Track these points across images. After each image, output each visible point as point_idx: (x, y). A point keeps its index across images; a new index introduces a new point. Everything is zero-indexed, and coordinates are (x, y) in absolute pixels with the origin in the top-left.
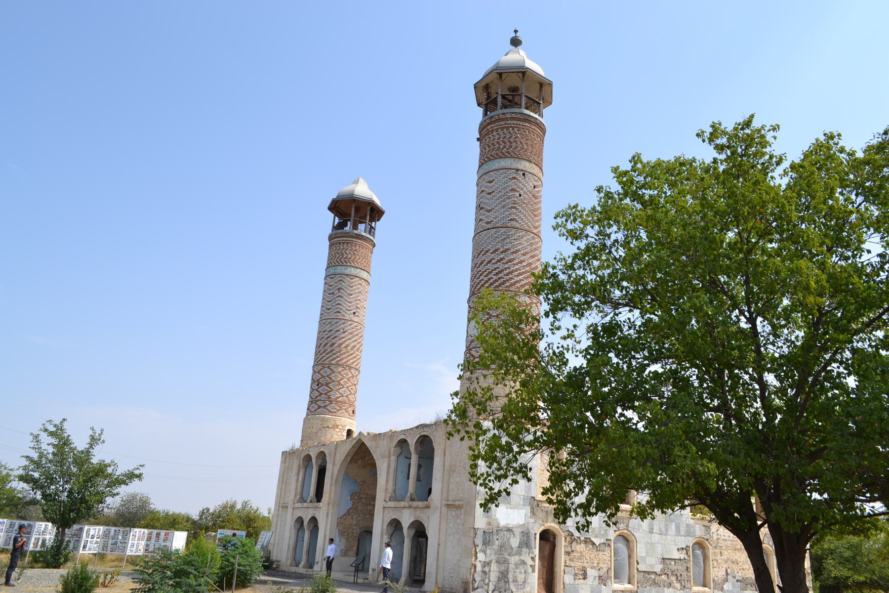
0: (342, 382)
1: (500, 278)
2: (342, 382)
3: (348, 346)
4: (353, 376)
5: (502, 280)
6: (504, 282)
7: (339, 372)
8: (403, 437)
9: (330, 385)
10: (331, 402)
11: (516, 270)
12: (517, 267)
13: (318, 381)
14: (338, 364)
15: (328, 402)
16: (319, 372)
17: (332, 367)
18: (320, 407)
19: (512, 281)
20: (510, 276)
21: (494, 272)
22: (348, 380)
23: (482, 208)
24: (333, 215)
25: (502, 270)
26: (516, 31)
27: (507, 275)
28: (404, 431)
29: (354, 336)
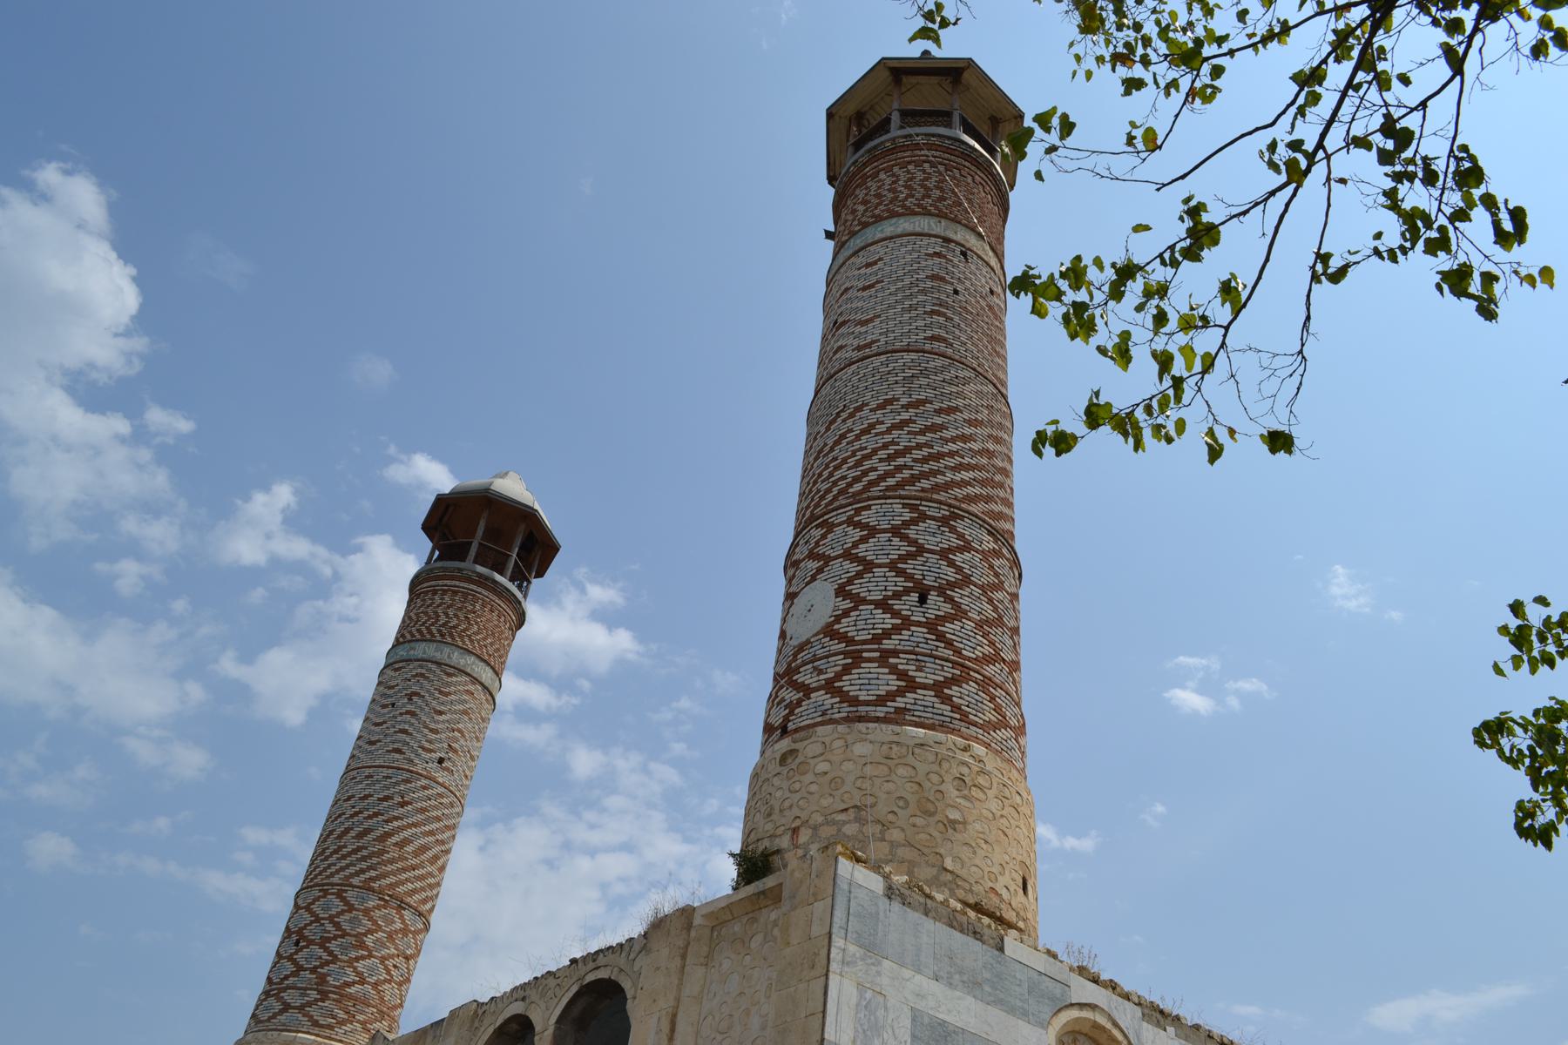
0: (369, 940)
1: (899, 469)
2: (369, 940)
3: (406, 842)
4: (405, 931)
5: (906, 474)
6: (913, 480)
7: (367, 912)
8: (517, 1008)
9: (333, 945)
10: (324, 996)
11: (951, 454)
12: (952, 447)
14: (367, 887)
15: (314, 995)
17: (350, 895)
18: (287, 1007)
19: (940, 479)
20: (933, 465)
21: (882, 454)
22: (390, 937)
24: (430, 545)
25: (908, 450)
27: (925, 460)
28: (524, 986)
29: (428, 821)
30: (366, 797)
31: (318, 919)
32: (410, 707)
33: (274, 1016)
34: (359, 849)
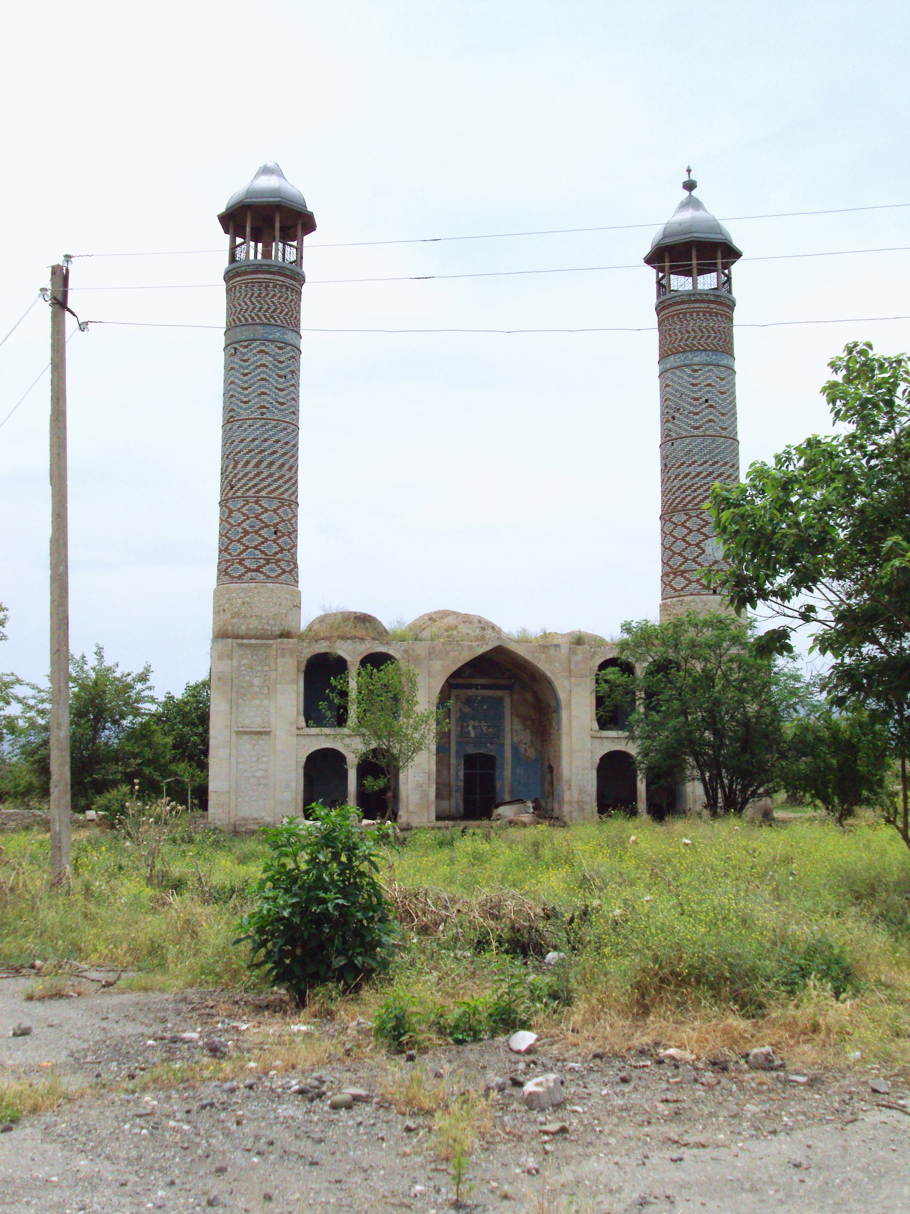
13: (275, 525)
16: (275, 511)
18: (284, 572)
23: (711, 406)
26: (689, 171)
30: (287, 443)
31: (283, 521)
32: (293, 382)
33: (279, 575)
34: (291, 478)
